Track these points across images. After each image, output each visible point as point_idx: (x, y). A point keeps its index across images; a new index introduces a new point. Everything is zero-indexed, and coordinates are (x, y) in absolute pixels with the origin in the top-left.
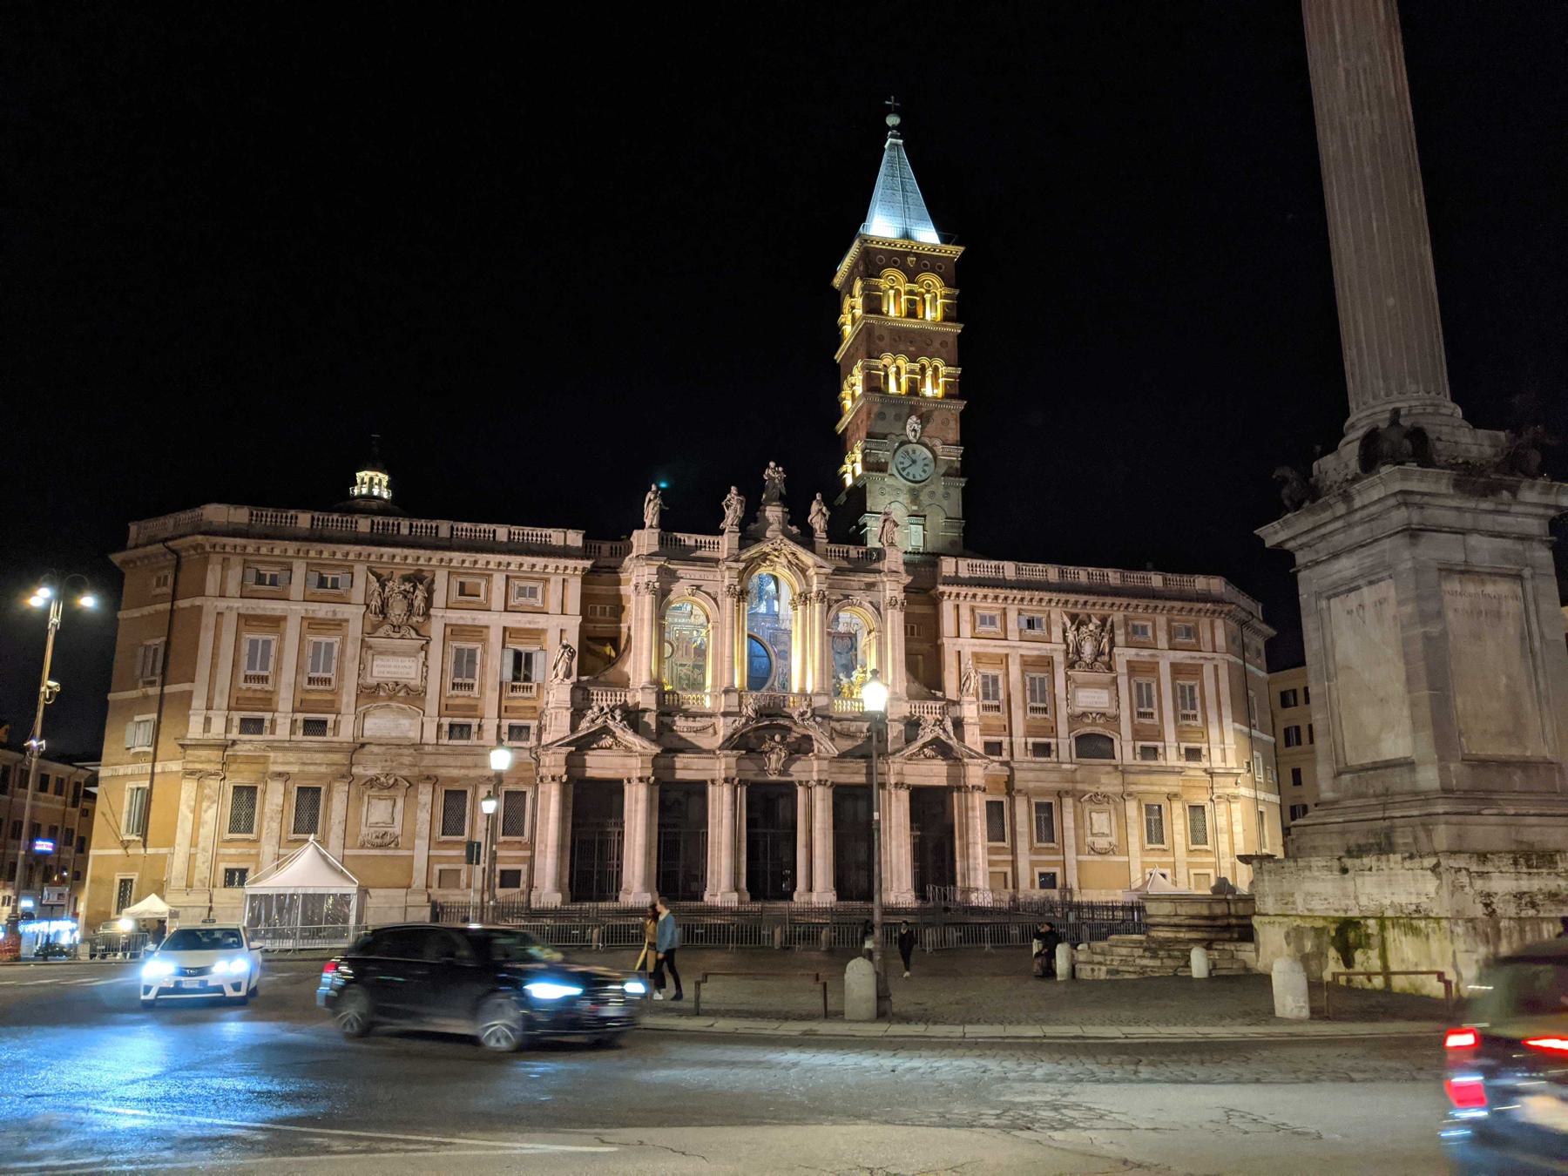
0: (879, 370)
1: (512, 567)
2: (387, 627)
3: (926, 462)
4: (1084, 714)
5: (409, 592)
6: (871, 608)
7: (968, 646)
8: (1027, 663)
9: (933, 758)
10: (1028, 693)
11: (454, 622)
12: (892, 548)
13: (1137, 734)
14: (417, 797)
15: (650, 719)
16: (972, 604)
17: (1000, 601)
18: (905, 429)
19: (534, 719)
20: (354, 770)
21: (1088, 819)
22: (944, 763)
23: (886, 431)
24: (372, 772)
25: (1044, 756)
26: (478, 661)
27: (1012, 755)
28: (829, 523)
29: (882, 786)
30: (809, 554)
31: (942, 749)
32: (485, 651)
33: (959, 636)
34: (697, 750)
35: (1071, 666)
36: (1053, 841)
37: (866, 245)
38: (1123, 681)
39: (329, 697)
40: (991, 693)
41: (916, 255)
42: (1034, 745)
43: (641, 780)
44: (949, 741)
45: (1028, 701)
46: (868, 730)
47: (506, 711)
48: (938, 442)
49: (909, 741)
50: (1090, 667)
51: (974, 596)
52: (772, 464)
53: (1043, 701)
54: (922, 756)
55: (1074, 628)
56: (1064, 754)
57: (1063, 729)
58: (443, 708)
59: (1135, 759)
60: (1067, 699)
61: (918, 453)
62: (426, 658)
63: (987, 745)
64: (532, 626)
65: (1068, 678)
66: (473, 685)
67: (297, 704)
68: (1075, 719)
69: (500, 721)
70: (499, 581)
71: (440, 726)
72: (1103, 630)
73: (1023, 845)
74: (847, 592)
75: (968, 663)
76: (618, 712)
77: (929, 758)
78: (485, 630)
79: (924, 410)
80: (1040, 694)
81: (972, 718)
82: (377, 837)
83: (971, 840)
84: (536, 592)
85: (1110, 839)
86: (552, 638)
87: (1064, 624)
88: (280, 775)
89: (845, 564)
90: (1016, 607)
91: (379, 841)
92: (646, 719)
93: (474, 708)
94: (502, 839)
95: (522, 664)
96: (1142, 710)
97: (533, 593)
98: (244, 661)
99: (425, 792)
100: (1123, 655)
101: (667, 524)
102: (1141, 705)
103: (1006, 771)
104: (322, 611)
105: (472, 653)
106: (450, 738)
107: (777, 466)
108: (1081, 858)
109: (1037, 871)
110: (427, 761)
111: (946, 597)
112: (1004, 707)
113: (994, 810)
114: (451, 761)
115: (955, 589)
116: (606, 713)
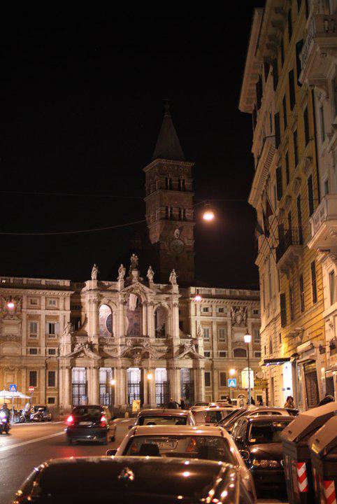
4: (237, 342)
8: (219, 324)
15: (96, 347)
31: (191, 356)
32: (40, 324)
34: (112, 357)
35: (233, 325)
43: (94, 368)
49: (180, 353)
50: (240, 325)
57: (230, 347)
63: (205, 353)
65: (232, 329)
68: (234, 344)
71: (27, 350)
73: (216, 387)
75: (199, 323)
76: (87, 346)
80: (222, 335)
86: (61, 319)
89: (159, 291)
93: (37, 343)
95: (52, 328)
100: (250, 320)
101: (99, 278)
103: (210, 362)
105: (36, 324)
110: (23, 362)
113: (207, 375)
114: (31, 361)
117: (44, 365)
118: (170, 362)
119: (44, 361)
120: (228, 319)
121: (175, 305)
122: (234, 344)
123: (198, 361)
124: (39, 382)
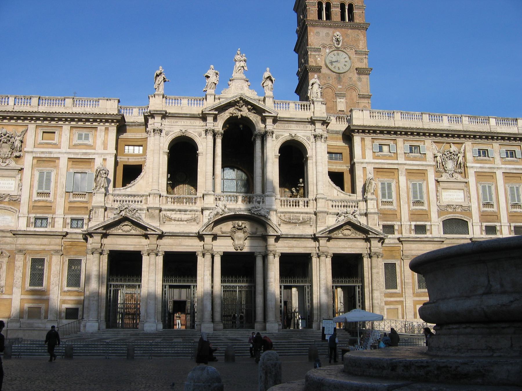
4: (448, 205)
19: (87, 214)
32: (57, 174)
57: (434, 215)
59: (482, 234)
63: (384, 226)
65: (438, 182)
66: (50, 193)
71: (28, 219)
73: (409, 291)
78: (57, 161)
84: (88, 137)
90: (402, 139)
94: (66, 289)
97: (87, 137)
99: (19, 260)
105: (49, 174)
106: (35, 227)
124: (49, 278)
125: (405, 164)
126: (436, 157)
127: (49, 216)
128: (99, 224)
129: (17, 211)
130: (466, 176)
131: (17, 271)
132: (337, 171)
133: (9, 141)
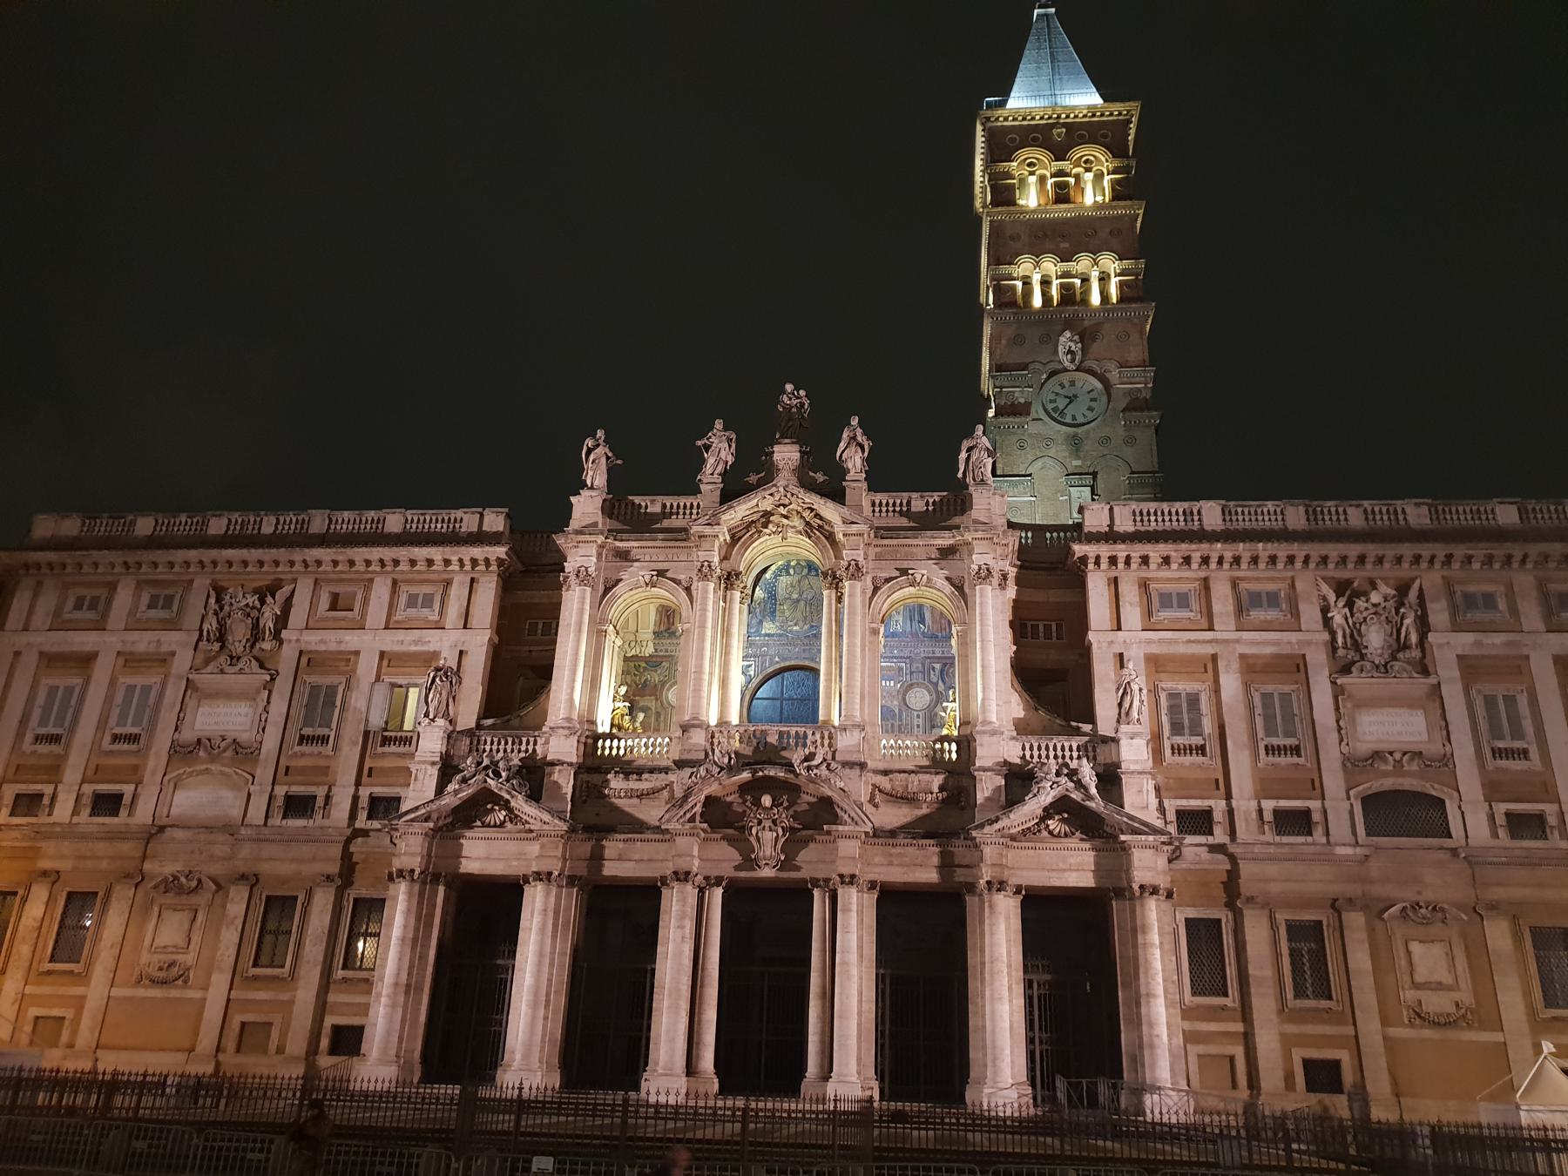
0: (1014, 279)
1: (404, 567)
2: (223, 659)
3: (1092, 395)
4: (1377, 755)
5: (253, 608)
6: (948, 588)
7: (1136, 641)
8: (1252, 669)
9: (1066, 835)
10: (1259, 721)
11: (312, 647)
12: (980, 488)
13: (1493, 790)
14: (224, 906)
16: (1144, 574)
17: (1195, 566)
18: (1056, 352)
20: (147, 866)
21: (1402, 953)
22: (1087, 845)
23: (1026, 361)
24: (169, 869)
25: (1303, 834)
26: (338, 703)
27: (1233, 833)
28: (868, 461)
29: (971, 887)
30: (830, 504)
33: (1119, 629)
34: (637, 826)
36: (1330, 998)
37: (989, 124)
38: (1453, 695)
39: (132, 761)
40: (1186, 722)
41: (1065, 125)
42: (1276, 812)
44: (1091, 804)
45: (1261, 734)
46: (942, 789)
47: (370, 775)
48: (1112, 366)
50: (1384, 669)
51: (1145, 560)
52: (789, 387)
53: (1290, 733)
54: (1045, 833)
55: (1341, 603)
56: (1339, 827)
57: (1333, 781)
58: (282, 770)
59: (1495, 835)
60: (1340, 729)
61: (1079, 384)
62: (268, 702)
63: (1181, 814)
64: (419, 648)
65: (1338, 692)
67: (90, 773)
68: (1357, 765)
69: (357, 790)
70: (381, 591)
72: (1400, 604)
73: (1264, 1004)
74: (905, 565)
77: (1059, 836)
79: (1086, 323)
81: (1136, 762)
82: (161, 969)
83: (1143, 990)
84: (432, 601)
85: (1456, 996)
87: (1324, 598)
88: (45, 873)
91: (162, 975)
92: (555, 777)
93: (325, 770)
94: (340, 974)
96: (1501, 744)
97: (428, 601)
98: (36, 714)
102: (1496, 733)
104: (143, 642)
105: (332, 691)
106: (284, 818)
107: (797, 389)
108: (1393, 1031)
109: (1298, 1055)
110: (246, 851)
111: (1091, 566)
112: (1213, 747)
115: (1105, 550)
116: (486, 768)
117: (334, 869)
118: (959, 850)
119: (336, 851)
120: (1309, 639)
121: (985, 575)
122: (1357, 765)
123: (1125, 849)
124: (299, 944)
125: (1237, 641)
126: (1327, 622)
127: (321, 792)
128: (417, 808)
129: (248, 780)
130: (1431, 669)
131: (228, 928)
132: (1049, 667)
133: (249, 615)
